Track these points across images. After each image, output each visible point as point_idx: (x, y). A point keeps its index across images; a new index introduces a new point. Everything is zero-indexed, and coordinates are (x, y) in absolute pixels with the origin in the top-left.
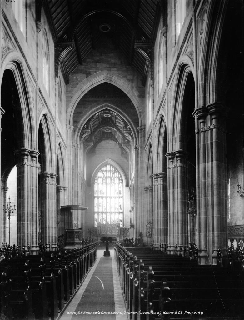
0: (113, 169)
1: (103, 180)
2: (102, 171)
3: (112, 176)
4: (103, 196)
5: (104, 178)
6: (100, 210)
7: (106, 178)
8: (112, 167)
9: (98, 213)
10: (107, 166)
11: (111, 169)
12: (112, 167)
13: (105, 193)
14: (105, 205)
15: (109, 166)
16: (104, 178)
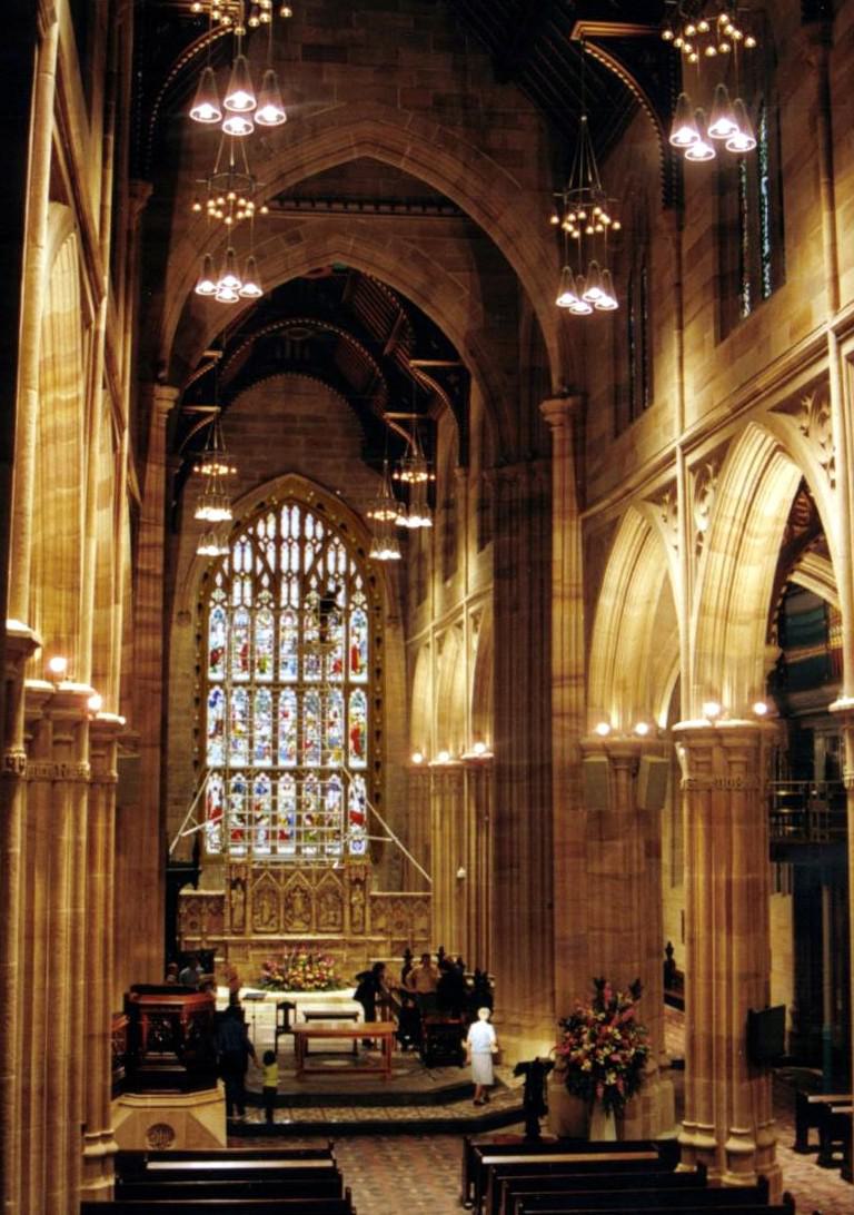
0: (320, 532)
1: (257, 587)
2: (254, 539)
3: (313, 569)
4: (258, 677)
5: (265, 581)
6: (238, 762)
7: (276, 578)
8: (309, 519)
9: (226, 773)
10: (285, 510)
11: (309, 533)
12: (309, 519)
13: (269, 664)
14: (267, 731)
15: (296, 512)
16: (265, 581)
